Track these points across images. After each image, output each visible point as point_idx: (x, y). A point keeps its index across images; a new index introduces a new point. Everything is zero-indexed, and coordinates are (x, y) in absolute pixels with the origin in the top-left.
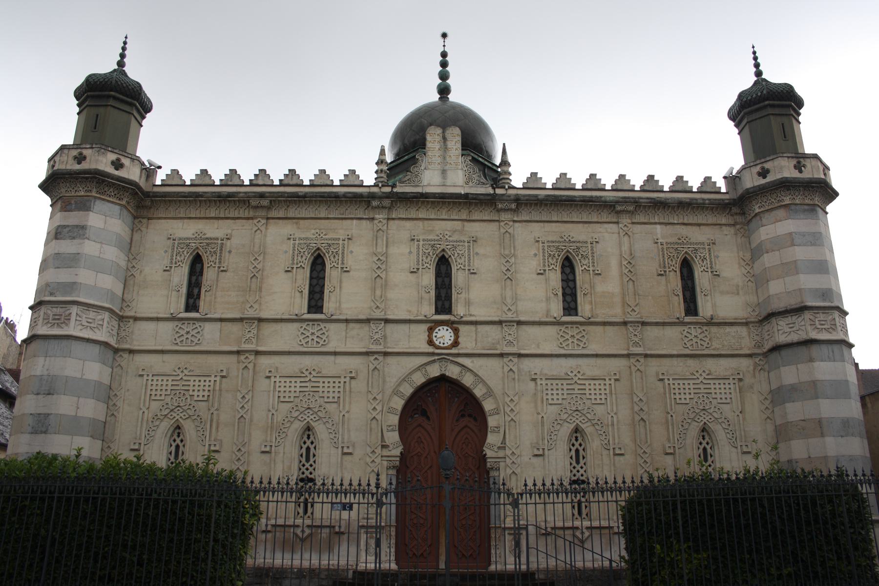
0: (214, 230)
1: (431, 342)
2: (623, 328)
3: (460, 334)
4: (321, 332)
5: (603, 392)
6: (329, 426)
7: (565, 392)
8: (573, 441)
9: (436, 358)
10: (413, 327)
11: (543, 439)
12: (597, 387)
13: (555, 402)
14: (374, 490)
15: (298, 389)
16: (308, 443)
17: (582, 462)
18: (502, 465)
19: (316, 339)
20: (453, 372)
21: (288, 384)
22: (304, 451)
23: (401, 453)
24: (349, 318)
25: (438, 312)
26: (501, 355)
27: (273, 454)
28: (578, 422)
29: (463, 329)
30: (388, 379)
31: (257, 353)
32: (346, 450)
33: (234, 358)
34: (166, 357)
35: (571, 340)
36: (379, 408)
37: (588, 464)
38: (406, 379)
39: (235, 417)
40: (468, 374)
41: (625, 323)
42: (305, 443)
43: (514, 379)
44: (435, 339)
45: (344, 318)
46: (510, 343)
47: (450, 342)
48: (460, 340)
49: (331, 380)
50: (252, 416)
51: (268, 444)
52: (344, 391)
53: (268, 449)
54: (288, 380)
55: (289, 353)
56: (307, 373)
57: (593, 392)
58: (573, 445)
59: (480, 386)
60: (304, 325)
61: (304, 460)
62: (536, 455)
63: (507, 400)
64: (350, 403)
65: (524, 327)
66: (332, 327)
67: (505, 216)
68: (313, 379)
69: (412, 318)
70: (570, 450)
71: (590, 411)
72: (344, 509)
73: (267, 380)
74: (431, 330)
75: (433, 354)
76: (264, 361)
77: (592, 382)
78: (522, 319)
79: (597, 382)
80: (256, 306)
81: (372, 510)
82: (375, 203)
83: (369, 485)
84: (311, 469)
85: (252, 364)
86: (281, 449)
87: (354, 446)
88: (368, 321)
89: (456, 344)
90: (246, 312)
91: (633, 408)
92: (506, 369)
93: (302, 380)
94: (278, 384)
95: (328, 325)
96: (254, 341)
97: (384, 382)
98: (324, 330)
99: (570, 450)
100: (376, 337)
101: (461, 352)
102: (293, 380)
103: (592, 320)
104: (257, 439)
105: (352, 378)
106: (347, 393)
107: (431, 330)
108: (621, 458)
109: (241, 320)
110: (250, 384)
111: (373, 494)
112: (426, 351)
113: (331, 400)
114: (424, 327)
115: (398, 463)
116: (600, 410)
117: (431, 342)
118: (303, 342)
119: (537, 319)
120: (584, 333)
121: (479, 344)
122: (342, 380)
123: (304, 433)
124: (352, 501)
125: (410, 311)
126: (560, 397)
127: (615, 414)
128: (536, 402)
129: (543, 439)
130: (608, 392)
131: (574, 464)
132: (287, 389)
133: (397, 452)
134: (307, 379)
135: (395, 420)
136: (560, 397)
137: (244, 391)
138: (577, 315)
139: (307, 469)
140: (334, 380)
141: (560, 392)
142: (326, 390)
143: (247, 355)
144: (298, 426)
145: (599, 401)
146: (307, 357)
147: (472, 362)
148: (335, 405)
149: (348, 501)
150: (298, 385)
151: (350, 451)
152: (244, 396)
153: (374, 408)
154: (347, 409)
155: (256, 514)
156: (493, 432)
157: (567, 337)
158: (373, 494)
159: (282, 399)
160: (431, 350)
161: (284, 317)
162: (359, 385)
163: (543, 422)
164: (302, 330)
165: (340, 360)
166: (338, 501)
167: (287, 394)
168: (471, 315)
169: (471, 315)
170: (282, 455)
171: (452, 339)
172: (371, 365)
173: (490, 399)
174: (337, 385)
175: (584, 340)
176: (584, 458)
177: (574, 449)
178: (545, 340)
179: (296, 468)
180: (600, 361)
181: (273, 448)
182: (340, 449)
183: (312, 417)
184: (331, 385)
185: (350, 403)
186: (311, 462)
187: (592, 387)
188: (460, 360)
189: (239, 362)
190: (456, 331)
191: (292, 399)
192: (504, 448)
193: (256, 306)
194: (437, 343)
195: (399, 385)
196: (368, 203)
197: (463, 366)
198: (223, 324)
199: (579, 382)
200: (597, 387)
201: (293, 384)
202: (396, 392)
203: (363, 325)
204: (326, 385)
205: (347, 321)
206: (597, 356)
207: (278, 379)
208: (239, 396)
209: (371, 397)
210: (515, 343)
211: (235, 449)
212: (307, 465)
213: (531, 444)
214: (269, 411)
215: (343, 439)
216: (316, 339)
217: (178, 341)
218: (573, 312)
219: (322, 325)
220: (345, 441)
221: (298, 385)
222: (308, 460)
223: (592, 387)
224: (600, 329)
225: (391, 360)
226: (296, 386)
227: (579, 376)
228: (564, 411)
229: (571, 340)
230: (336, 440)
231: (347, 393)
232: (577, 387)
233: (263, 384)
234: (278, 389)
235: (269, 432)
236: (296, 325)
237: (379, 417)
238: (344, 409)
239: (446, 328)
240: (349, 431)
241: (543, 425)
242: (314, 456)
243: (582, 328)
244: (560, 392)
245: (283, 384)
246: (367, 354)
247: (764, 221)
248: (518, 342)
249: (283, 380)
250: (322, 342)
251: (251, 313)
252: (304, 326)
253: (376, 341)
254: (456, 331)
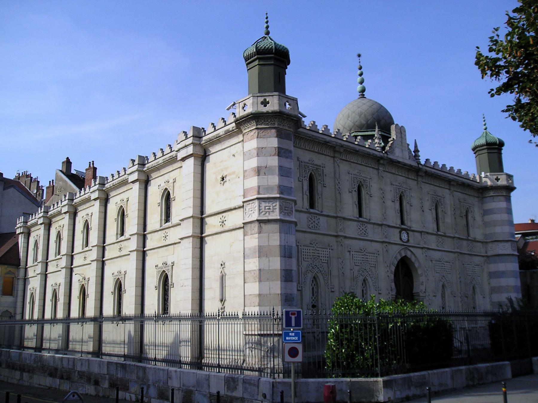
0: (319, 160)
1: (401, 239)
20: (409, 254)
33: (334, 239)
34: (307, 235)
67: (420, 179)
74: (400, 232)
76: (347, 242)
82: (382, 162)
88: (381, 225)
89: (408, 241)
114: (398, 230)
117: (401, 239)
165: (374, 244)
188: (410, 248)
196: (378, 161)
198: (328, 218)
205: (374, 224)
217: (311, 226)
247: (495, 200)
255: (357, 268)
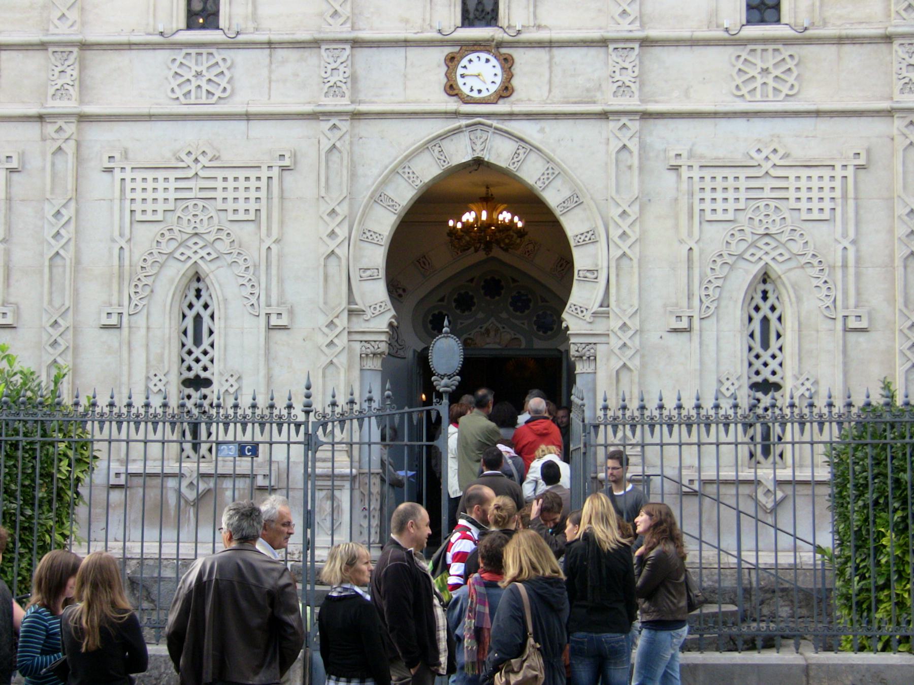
1: (451, 89)
2: (883, 47)
3: (516, 69)
4: (217, 70)
5: (827, 194)
6: (240, 270)
7: (742, 195)
8: (758, 300)
9: (464, 122)
10: (414, 53)
11: (690, 297)
12: (815, 184)
13: (720, 216)
14: (301, 417)
15: (172, 195)
16: (198, 306)
17: (774, 344)
18: (601, 350)
19: (205, 87)
20: (500, 153)
21: (150, 185)
22: (189, 323)
23: (391, 325)
24: (275, 38)
25: (468, 20)
26: (604, 115)
27: (125, 331)
28: (767, 259)
29: (519, 56)
30: (360, 171)
31: (83, 118)
32: (274, 321)
35: (760, 80)
36: (342, 232)
37: (787, 349)
38: (400, 169)
39: (42, 255)
40: (533, 156)
41: (888, 39)
42: (191, 306)
43: (630, 167)
44: (460, 81)
45: (264, 38)
46: (622, 89)
47: (493, 88)
48: (515, 82)
49: (241, 174)
50: (78, 251)
51: (115, 310)
52: (269, 198)
53: (114, 320)
54: (150, 175)
55: (150, 117)
56: (189, 161)
57: (804, 194)
58: (757, 309)
59: (558, 183)
60: (179, 55)
61: (189, 341)
62: (675, 330)
63: (615, 212)
64: (282, 223)
65: (656, 51)
66: (240, 57)
68: (202, 174)
69: (410, 36)
70: (750, 319)
71: (796, 236)
72: (242, 453)
73: (106, 176)
74: (452, 60)
75: (456, 114)
76: (97, 135)
77: (804, 173)
78: (653, 33)
79: (815, 173)
80: (73, 15)
81: (298, 452)
83: (290, 407)
84: (205, 360)
85: (72, 143)
86: (141, 320)
87: (291, 312)
88: (316, 44)
89: (506, 91)
90: (52, 29)
91: (891, 231)
92: (615, 145)
93: (180, 174)
94: (129, 185)
95: (229, 54)
96: (74, 92)
97: (353, 176)
98: (223, 67)
99: (750, 319)
100: (333, 80)
101: (516, 109)
102: (161, 175)
103: (808, 33)
104: (95, 300)
105: (284, 169)
106: (276, 201)
107: (452, 60)
108: (861, 337)
109: (43, 46)
110: (70, 185)
111: (298, 425)
112: (442, 107)
113: (241, 216)
115: (384, 347)
116: (819, 234)
117: (451, 89)
118: (179, 93)
119: (686, 34)
120: (790, 64)
121: (556, 92)
122: (264, 174)
123: (188, 287)
124: (258, 438)
125: (407, 21)
126: (731, 205)
127: (854, 242)
128: (676, 218)
129: (690, 297)
130: (838, 194)
131: (758, 349)
132: (150, 195)
133: (382, 323)
134: (190, 174)
135: (377, 256)
136: (731, 205)
137: (59, 202)
138: (778, 21)
139: (197, 360)
140: (247, 173)
141: (731, 195)
142: (230, 195)
143: (60, 123)
144: (175, 272)
145: (816, 215)
146: (189, 124)
147: (542, 130)
148: (251, 227)
149: (248, 438)
150: (172, 185)
151: (283, 321)
152: (58, 212)
153: (332, 234)
154: (275, 235)
155: (84, 462)
156: (585, 280)
157: (752, 72)
158: (298, 425)
159: (139, 216)
160: (452, 105)
161: (135, 39)
162: (302, 184)
163: (690, 260)
164: (175, 67)
165: (259, 128)
166: (230, 437)
167: (149, 206)
168: (539, 27)
169: (539, 27)
170: (143, 331)
171: (498, 80)
172: (324, 141)
173: (577, 211)
174: (253, 184)
175: (791, 79)
176: (779, 336)
177: (757, 317)
178: (703, 79)
179: (175, 359)
180: (824, 125)
181: (125, 319)
182: (263, 318)
183: (203, 253)
184: (242, 184)
185: (282, 223)
186: (205, 345)
187: (803, 183)
188: (514, 127)
189: (44, 139)
190: (507, 63)
191: (159, 217)
192: (606, 315)
193: (73, 15)
194: (466, 90)
195: (385, 182)
197: (522, 140)
199: (773, 172)
200: (815, 184)
201: (161, 185)
202: (378, 198)
203: (306, 53)
204: (231, 184)
205: (270, 45)
206: (818, 114)
207: (128, 175)
208: (49, 211)
209: (325, 208)
210: (634, 87)
211: (46, 321)
212: (197, 352)
213: (665, 306)
214: (113, 240)
215: (268, 296)
216: (205, 87)
218: (769, 14)
219: (218, 56)
220: (274, 301)
221: (172, 185)
222: (197, 341)
223: (803, 183)
224: (830, 51)
225: (365, 128)
226: (166, 188)
227: (775, 159)
228: (738, 236)
229: (760, 80)
230: (253, 300)
231: (276, 201)
232: (770, 183)
233: (100, 186)
234: (129, 195)
235: (115, 287)
236: (163, 55)
237: (342, 252)
238: (269, 235)
239: (484, 56)
240: (281, 281)
241: (690, 268)
242: (211, 332)
243: (786, 51)
244: (731, 195)
245: (139, 185)
246: (314, 116)
248: (642, 85)
249: (139, 175)
250: (218, 93)
251: (62, 32)
252: (180, 59)
253: (334, 90)
254: (507, 63)
255: (145, 235)
